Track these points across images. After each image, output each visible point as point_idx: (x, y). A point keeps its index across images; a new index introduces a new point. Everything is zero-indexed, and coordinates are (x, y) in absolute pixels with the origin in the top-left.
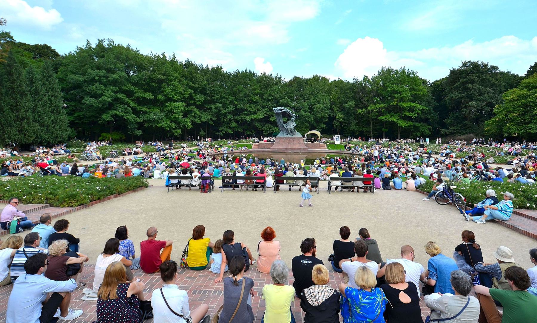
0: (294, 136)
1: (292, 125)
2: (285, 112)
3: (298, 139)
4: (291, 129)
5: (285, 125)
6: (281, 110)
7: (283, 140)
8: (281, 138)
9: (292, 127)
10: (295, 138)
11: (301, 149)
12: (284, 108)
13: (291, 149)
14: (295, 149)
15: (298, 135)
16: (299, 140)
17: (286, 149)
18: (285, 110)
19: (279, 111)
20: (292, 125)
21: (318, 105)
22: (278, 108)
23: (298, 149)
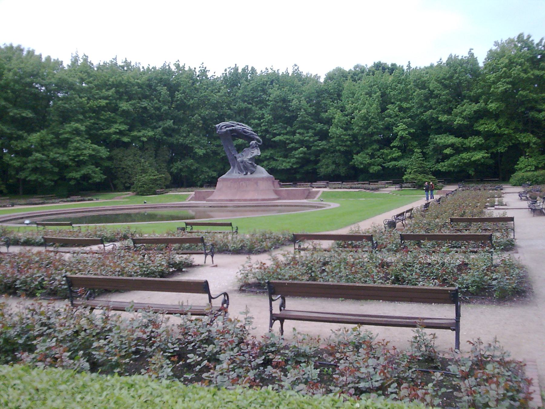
8: (224, 180)
10: (249, 180)
11: (257, 200)
14: (245, 200)
15: (262, 172)
16: (257, 183)
23: (251, 200)
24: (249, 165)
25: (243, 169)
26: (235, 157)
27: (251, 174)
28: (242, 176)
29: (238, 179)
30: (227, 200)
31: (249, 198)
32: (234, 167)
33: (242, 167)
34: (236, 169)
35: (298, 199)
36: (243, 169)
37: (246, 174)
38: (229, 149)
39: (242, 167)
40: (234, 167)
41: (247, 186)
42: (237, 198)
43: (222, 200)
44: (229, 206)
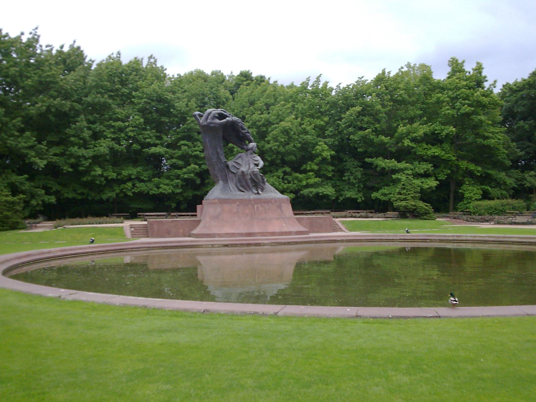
1: (250, 163)
2: (233, 123)
3: (279, 204)
6: (221, 116)
8: (222, 201)
10: (267, 201)
11: (289, 233)
14: (273, 234)
16: (280, 207)
19: (217, 121)
20: (250, 163)
24: (260, 177)
25: (251, 185)
26: (227, 167)
29: (250, 200)
30: (241, 235)
31: (277, 230)
32: (226, 181)
34: (232, 185)
35: (329, 232)
36: (251, 185)
37: (258, 193)
38: (217, 153)
39: (249, 182)
40: (226, 181)
42: (256, 230)
43: (233, 235)
44: (264, 245)
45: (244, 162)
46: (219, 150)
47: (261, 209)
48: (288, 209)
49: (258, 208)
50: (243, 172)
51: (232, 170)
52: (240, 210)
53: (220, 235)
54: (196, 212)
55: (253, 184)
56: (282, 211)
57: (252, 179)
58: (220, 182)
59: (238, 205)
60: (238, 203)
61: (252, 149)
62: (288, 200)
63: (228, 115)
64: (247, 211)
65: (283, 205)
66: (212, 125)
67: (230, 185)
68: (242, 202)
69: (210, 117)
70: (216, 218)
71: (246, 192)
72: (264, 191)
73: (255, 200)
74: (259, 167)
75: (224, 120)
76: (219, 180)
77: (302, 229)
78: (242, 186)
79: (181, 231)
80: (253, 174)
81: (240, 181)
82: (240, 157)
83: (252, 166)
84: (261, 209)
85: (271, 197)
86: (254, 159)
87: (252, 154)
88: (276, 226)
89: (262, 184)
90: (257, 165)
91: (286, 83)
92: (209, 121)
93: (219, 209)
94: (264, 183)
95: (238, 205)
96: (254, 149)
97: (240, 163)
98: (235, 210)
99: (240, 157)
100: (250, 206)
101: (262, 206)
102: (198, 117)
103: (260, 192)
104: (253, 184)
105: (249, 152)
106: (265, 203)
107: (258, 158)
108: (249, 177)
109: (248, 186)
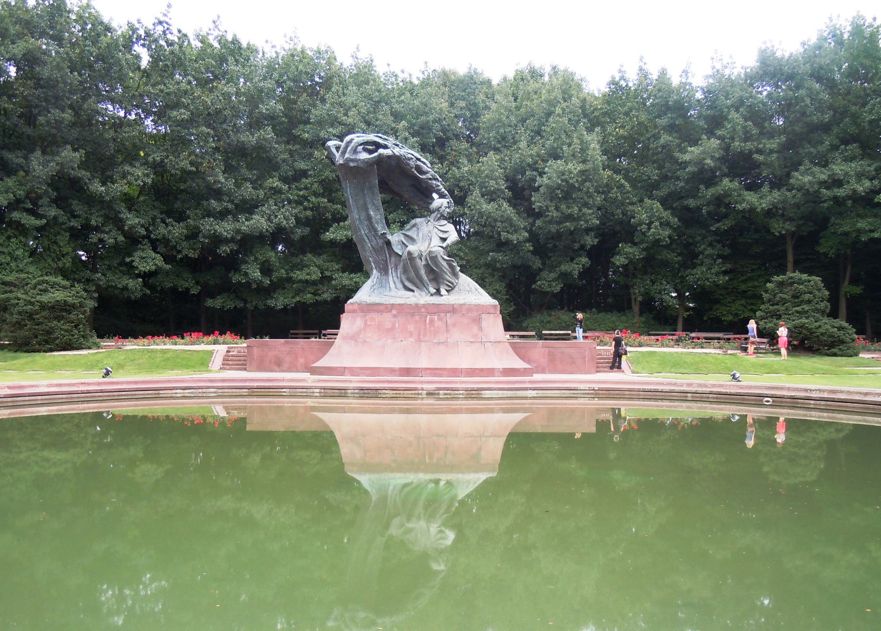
0: (447, 299)
1: (431, 236)
3: (475, 314)
4: (433, 258)
5: (395, 238)
7: (387, 319)
9: (436, 245)
10: (453, 309)
11: (490, 372)
12: (390, 141)
13: (435, 372)
14: (455, 372)
15: (470, 293)
16: (477, 321)
17: (407, 372)
18: (397, 151)
19: (364, 156)
21: (553, 167)
22: (357, 138)
23: (472, 372)
24: (444, 264)
25: (425, 278)
26: (388, 243)
27: (447, 291)
28: (420, 298)
30: (391, 371)
31: (465, 365)
32: (384, 271)
33: (423, 272)
34: (393, 279)
36: (425, 278)
37: (438, 292)
38: (369, 218)
39: (423, 272)
40: (384, 271)
41: (447, 331)
42: (423, 362)
43: (374, 371)
45: (420, 235)
46: (372, 213)
47: (438, 323)
48: (494, 325)
49: (432, 321)
50: (409, 253)
51: (396, 251)
52: (397, 325)
53: (353, 371)
54: (338, 328)
55: (431, 277)
56: (480, 329)
57: (427, 266)
58: (375, 271)
59: (395, 316)
60: (394, 312)
61: (438, 209)
62: (495, 306)
63: (390, 145)
64: (411, 327)
65: (483, 316)
66: (352, 164)
67: (390, 278)
68: (401, 309)
69: (349, 148)
70: (353, 338)
71: (417, 292)
72: (456, 289)
73: (424, 306)
74: (444, 245)
75: (376, 154)
76: (372, 269)
77: (519, 364)
78: (409, 280)
79: (302, 361)
80: (431, 258)
81: (405, 271)
82: (414, 226)
83: (436, 242)
84: (438, 323)
85: (461, 302)
86: (440, 228)
87: (439, 219)
88: (465, 357)
89: (449, 277)
90: (444, 240)
91: (596, 85)
92: (347, 156)
93: (359, 322)
94: (455, 275)
95: (395, 316)
96: (441, 210)
97: (415, 236)
98: (388, 325)
99: (414, 226)
100: (417, 318)
101: (440, 319)
102: (334, 150)
103: (443, 292)
104: (431, 277)
105: (433, 215)
106: (449, 312)
107: (450, 227)
108: (424, 263)
109: (421, 280)
